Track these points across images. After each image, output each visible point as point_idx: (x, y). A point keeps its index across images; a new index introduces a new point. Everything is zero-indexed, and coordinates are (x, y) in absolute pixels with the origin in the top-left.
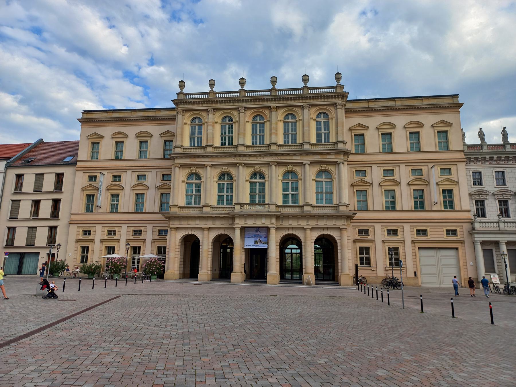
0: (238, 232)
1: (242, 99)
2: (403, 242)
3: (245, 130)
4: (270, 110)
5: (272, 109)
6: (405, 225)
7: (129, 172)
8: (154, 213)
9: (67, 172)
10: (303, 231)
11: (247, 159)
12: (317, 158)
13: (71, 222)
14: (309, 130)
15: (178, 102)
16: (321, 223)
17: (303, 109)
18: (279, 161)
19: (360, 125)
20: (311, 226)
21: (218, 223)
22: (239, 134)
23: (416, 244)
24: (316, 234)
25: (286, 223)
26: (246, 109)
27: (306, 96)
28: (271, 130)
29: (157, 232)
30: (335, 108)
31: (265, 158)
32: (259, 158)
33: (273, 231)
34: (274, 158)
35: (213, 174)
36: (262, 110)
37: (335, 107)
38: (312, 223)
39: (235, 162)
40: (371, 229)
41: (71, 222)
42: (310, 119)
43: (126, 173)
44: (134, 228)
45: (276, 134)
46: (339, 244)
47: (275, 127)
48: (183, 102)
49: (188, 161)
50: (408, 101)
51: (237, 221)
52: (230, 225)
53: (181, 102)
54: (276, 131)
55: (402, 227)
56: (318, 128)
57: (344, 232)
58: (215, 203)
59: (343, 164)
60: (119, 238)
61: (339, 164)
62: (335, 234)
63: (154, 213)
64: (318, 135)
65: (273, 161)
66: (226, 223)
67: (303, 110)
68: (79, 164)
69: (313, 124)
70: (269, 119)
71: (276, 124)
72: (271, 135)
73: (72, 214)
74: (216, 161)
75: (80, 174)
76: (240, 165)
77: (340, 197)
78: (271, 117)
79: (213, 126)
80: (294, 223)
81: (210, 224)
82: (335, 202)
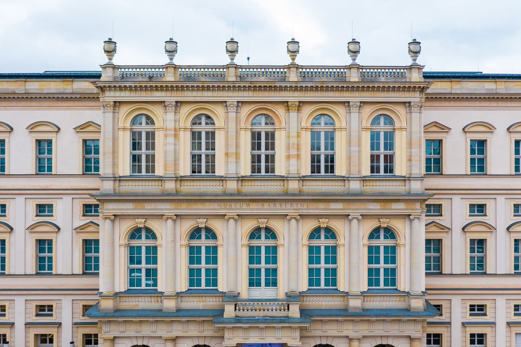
1: (232, 85)
2: (493, 324)
3: (237, 147)
4: (287, 108)
5: (290, 108)
6: (498, 298)
7: (20, 200)
11: (244, 206)
12: (375, 208)
14: (360, 152)
15: (105, 86)
17: (349, 110)
18: (305, 212)
19: (436, 124)
20: (360, 335)
22: (227, 154)
23: (512, 329)
26: (240, 104)
27: (356, 86)
28: (288, 148)
29: (80, 310)
30: (408, 111)
31: (278, 205)
32: (266, 205)
34: (295, 206)
35: (178, 232)
36: (269, 106)
37: (408, 109)
39: (222, 212)
40: (445, 305)
42: (361, 129)
43: (14, 199)
44: (37, 301)
45: (298, 156)
47: (296, 143)
48: (115, 87)
49: (128, 208)
50: (516, 83)
52: (215, 333)
53: (109, 87)
54: (298, 149)
55: (494, 302)
58: (183, 286)
59: (418, 218)
60: (11, 321)
61: (411, 221)
65: (293, 211)
67: (348, 111)
70: (283, 125)
71: (298, 136)
72: (288, 157)
74: (184, 209)
76: (230, 218)
78: (288, 123)
79: (176, 136)
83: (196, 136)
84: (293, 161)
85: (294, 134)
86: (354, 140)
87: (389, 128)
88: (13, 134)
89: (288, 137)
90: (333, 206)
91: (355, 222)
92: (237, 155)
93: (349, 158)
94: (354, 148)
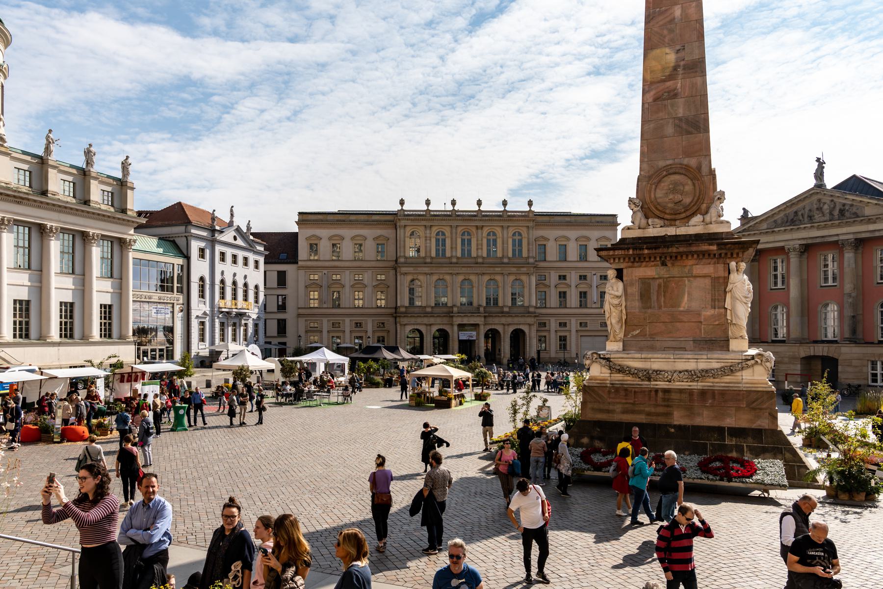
0: (456, 328)
3: (456, 245)
8: (372, 308)
9: (288, 268)
10: (502, 326)
13: (299, 315)
16: (516, 320)
21: (439, 320)
22: (452, 248)
24: (511, 329)
25: (490, 320)
28: (477, 245)
33: (482, 327)
38: (509, 320)
41: (299, 315)
45: (482, 249)
46: (528, 336)
51: (455, 319)
56: (514, 245)
57: (532, 327)
62: (525, 328)
63: (372, 308)
64: (514, 251)
66: (445, 320)
68: (300, 263)
69: (510, 241)
72: (477, 249)
73: (299, 308)
75: (302, 272)
77: (530, 301)
79: (430, 240)
80: (496, 320)
81: (432, 320)
82: (526, 304)
83: (437, 240)
84: (480, 251)
85: (480, 239)
86: (505, 242)
87: (520, 237)
88: (344, 241)
89: (477, 240)
90: (497, 269)
91: (506, 276)
92: (456, 248)
93: (503, 249)
94: (505, 245)
